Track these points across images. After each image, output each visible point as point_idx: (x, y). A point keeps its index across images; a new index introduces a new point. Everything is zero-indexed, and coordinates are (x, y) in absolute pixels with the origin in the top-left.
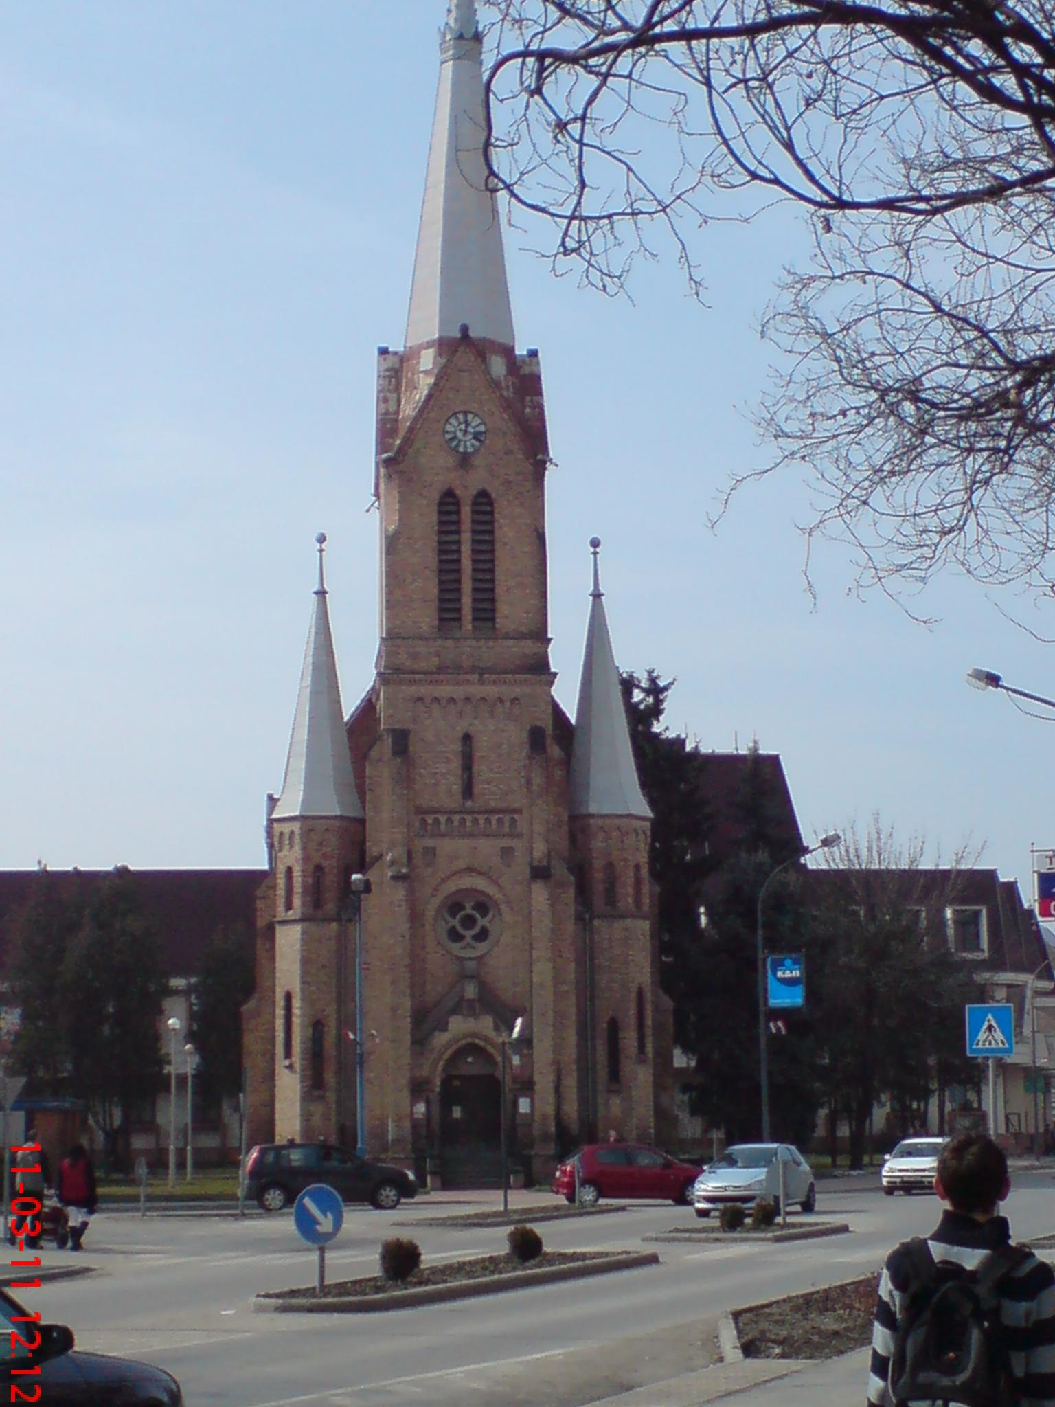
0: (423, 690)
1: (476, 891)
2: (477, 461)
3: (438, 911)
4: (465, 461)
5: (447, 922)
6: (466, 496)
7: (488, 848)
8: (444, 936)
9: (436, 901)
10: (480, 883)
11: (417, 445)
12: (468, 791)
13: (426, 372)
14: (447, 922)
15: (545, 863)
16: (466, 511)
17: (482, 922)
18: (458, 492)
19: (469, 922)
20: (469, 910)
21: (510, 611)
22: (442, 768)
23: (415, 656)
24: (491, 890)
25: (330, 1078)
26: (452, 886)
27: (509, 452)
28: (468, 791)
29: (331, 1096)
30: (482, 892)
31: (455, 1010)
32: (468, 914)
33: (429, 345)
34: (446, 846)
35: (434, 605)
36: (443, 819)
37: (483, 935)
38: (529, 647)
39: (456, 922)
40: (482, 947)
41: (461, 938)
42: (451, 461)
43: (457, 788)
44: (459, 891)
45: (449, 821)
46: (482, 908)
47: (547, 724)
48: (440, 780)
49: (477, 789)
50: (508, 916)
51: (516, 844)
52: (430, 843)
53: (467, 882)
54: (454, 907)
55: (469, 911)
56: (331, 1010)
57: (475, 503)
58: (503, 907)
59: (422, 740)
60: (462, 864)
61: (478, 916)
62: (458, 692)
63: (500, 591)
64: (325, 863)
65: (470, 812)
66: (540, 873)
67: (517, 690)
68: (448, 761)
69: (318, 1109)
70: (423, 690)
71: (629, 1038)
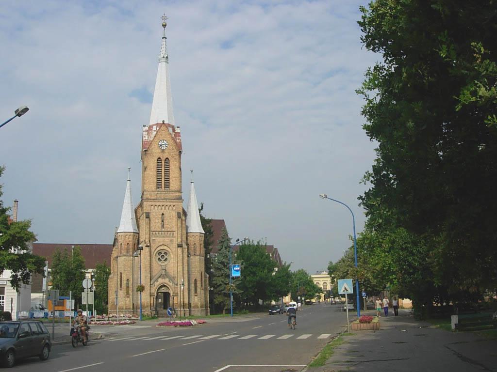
0: (153, 203)
2: (166, 151)
4: (163, 151)
6: (163, 159)
7: (167, 240)
10: (165, 248)
11: (153, 147)
12: (163, 226)
13: (154, 131)
15: (181, 244)
16: (163, 162)
17: (166, 257)
18: (161, 158)
21: (174, 185)
22: (157, 221)
23: (151, 196)
24: (168, 249)
25: (130, 292)
27: (173, 149)
28: (163, 226)
29: (131, 296)
32: (163, 255)
33: (155, 125)
35: (156, 184)
36: (157, 233)
37: (166, 260)
38: (177, 194)
39: (160, 257)
40: (166, 263)
42: (160, 151)
43: (160, 226)
45: (159, 233)
47: (181, 212)
48: (156, 224)
49: (165, 226)
50: (172, 256)
51: (174, 239)
55: (163, 254)
56: (131, 277)
57: (165, 161)
58: (171, 253)
59: (153, 215)
60: (161, 244)
62: (161, 204)
63: (171, 181)
64: (130, 243)
65: (163, 232)
66: (180, 246)
67: (174, 204)
68: (158, 220)
69: (128, 299)
70: (153, 203)
71: (199, 284)
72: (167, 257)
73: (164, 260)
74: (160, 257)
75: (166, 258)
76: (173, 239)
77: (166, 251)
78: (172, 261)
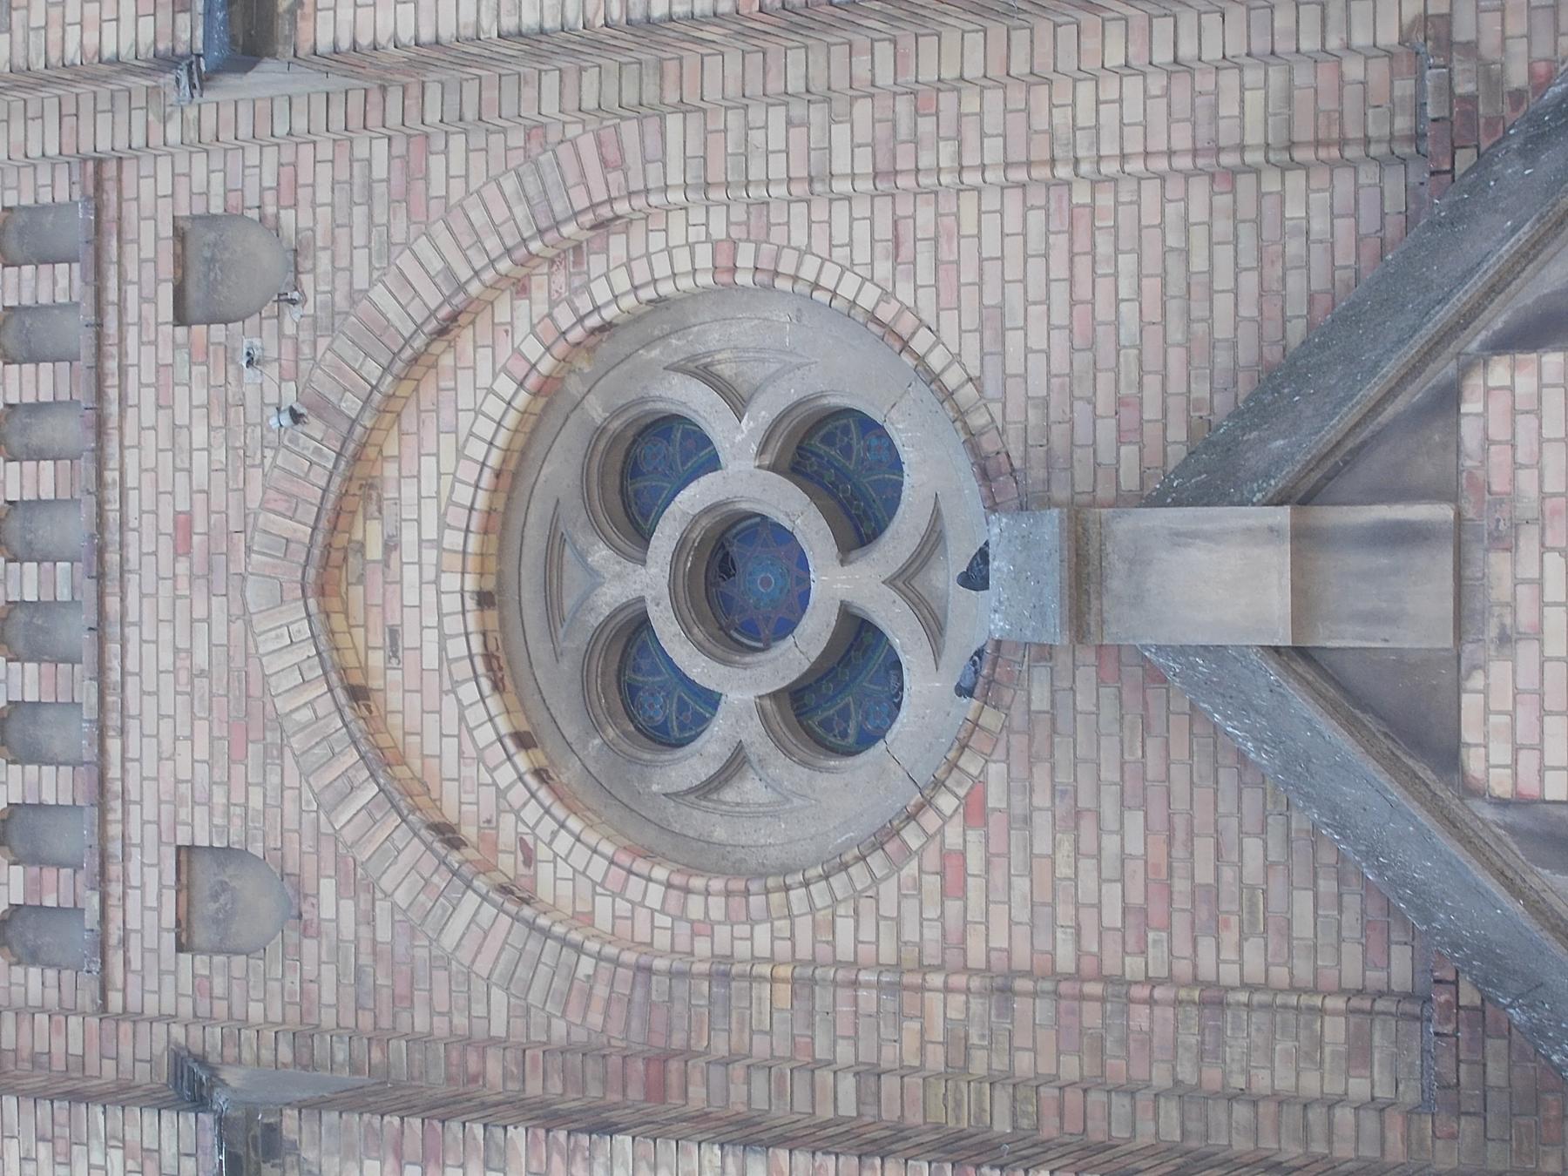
1: (498, 524)
3: (651, 839)
5: (736, 763)
8: (851, 790)
9: (572, 860)
10: (436, 486)
14: (736, 763)
17: (742, 475)
19: (734, 578)
20: (646, 580)
26: (457, 731)
30: (511, 478)
31: (1409, 722)
34: (173, 773)
37: (839, 461)
39: (742, 688)
40: (929, 470)
41: (858, 637)
44: (497, 667)
46: (645, 461)
50: (670, 252)
51: (151, 203)
52: (146, 900)
53: (425, 595)
54: (639, 697)
58: (610, 287)
60: (284, 642)
61: (694, 498)
72: (738, 439)
73: (859, 526)
74: (742, 688)
75: (634, 523)
76: (145, 258)
77: (560, 471)
78: (842, 250)
